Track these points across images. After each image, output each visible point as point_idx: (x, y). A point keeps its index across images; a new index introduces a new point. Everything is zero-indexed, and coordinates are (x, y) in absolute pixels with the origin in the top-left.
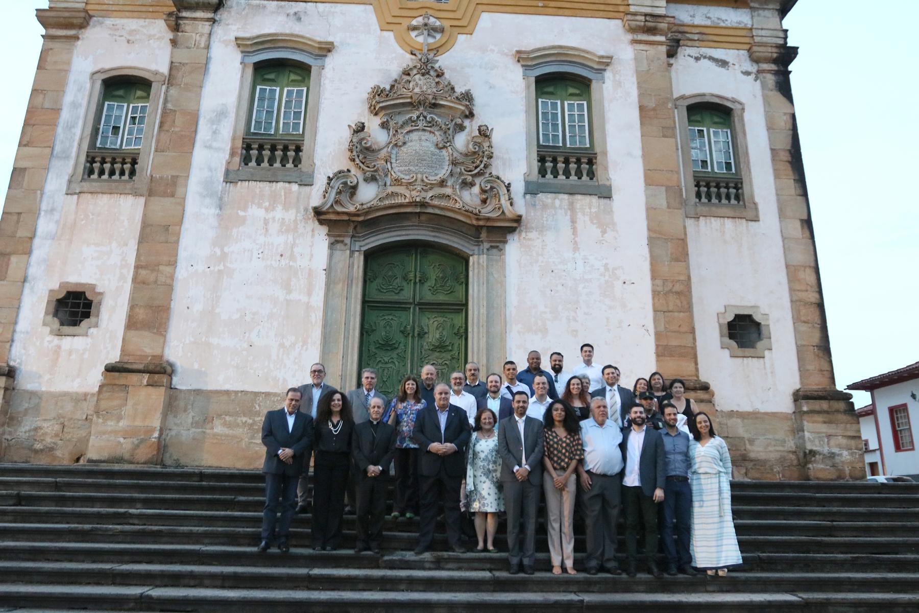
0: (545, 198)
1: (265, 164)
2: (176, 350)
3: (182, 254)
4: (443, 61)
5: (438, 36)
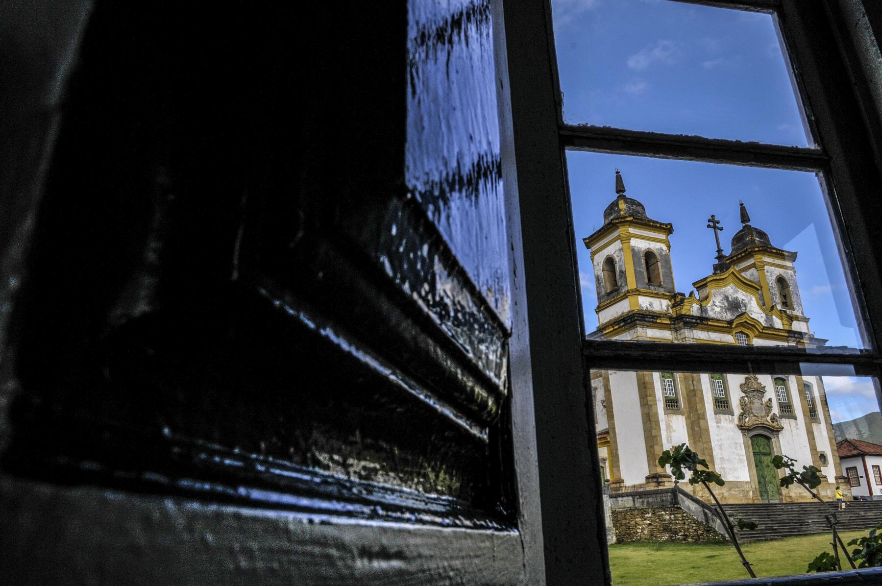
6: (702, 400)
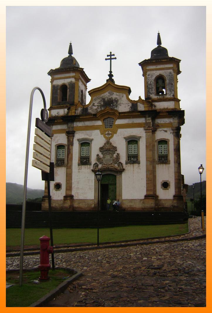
0: (129, 165)
2: (73, 193)
3: (73, 178)
4: (111, 140)
5: (111, 135)
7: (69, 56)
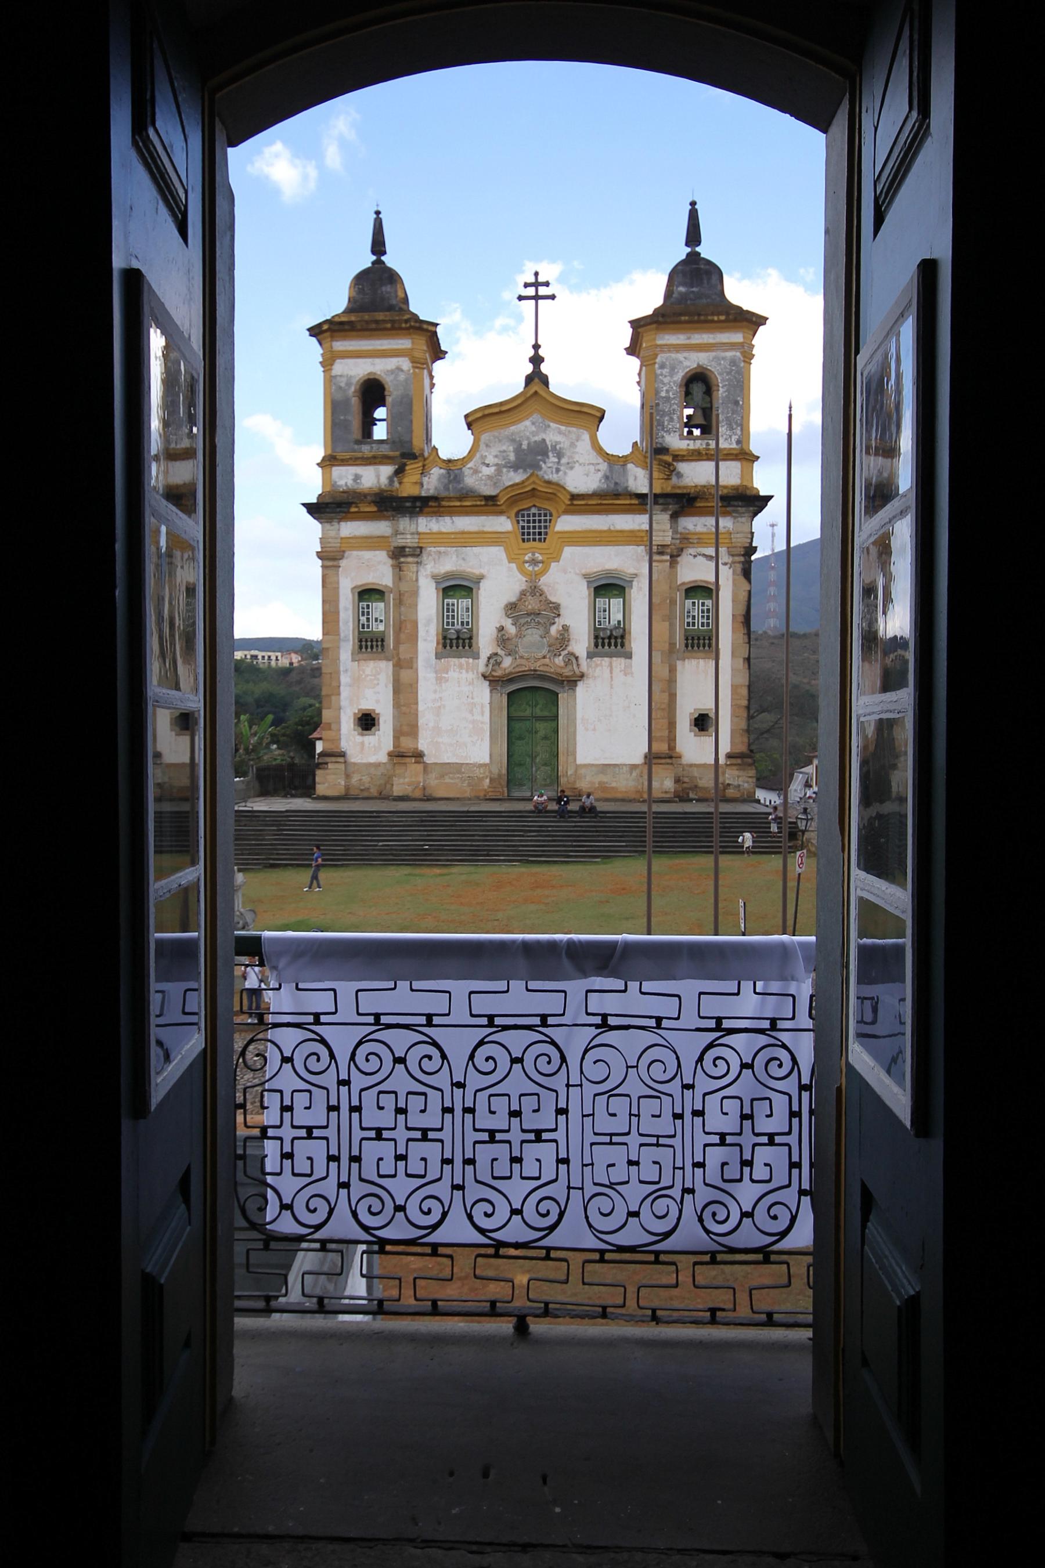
1: (454, 648)
2: (423, 745)
4: (544, 581)
6: (414, 638)
7: (373, 263)
